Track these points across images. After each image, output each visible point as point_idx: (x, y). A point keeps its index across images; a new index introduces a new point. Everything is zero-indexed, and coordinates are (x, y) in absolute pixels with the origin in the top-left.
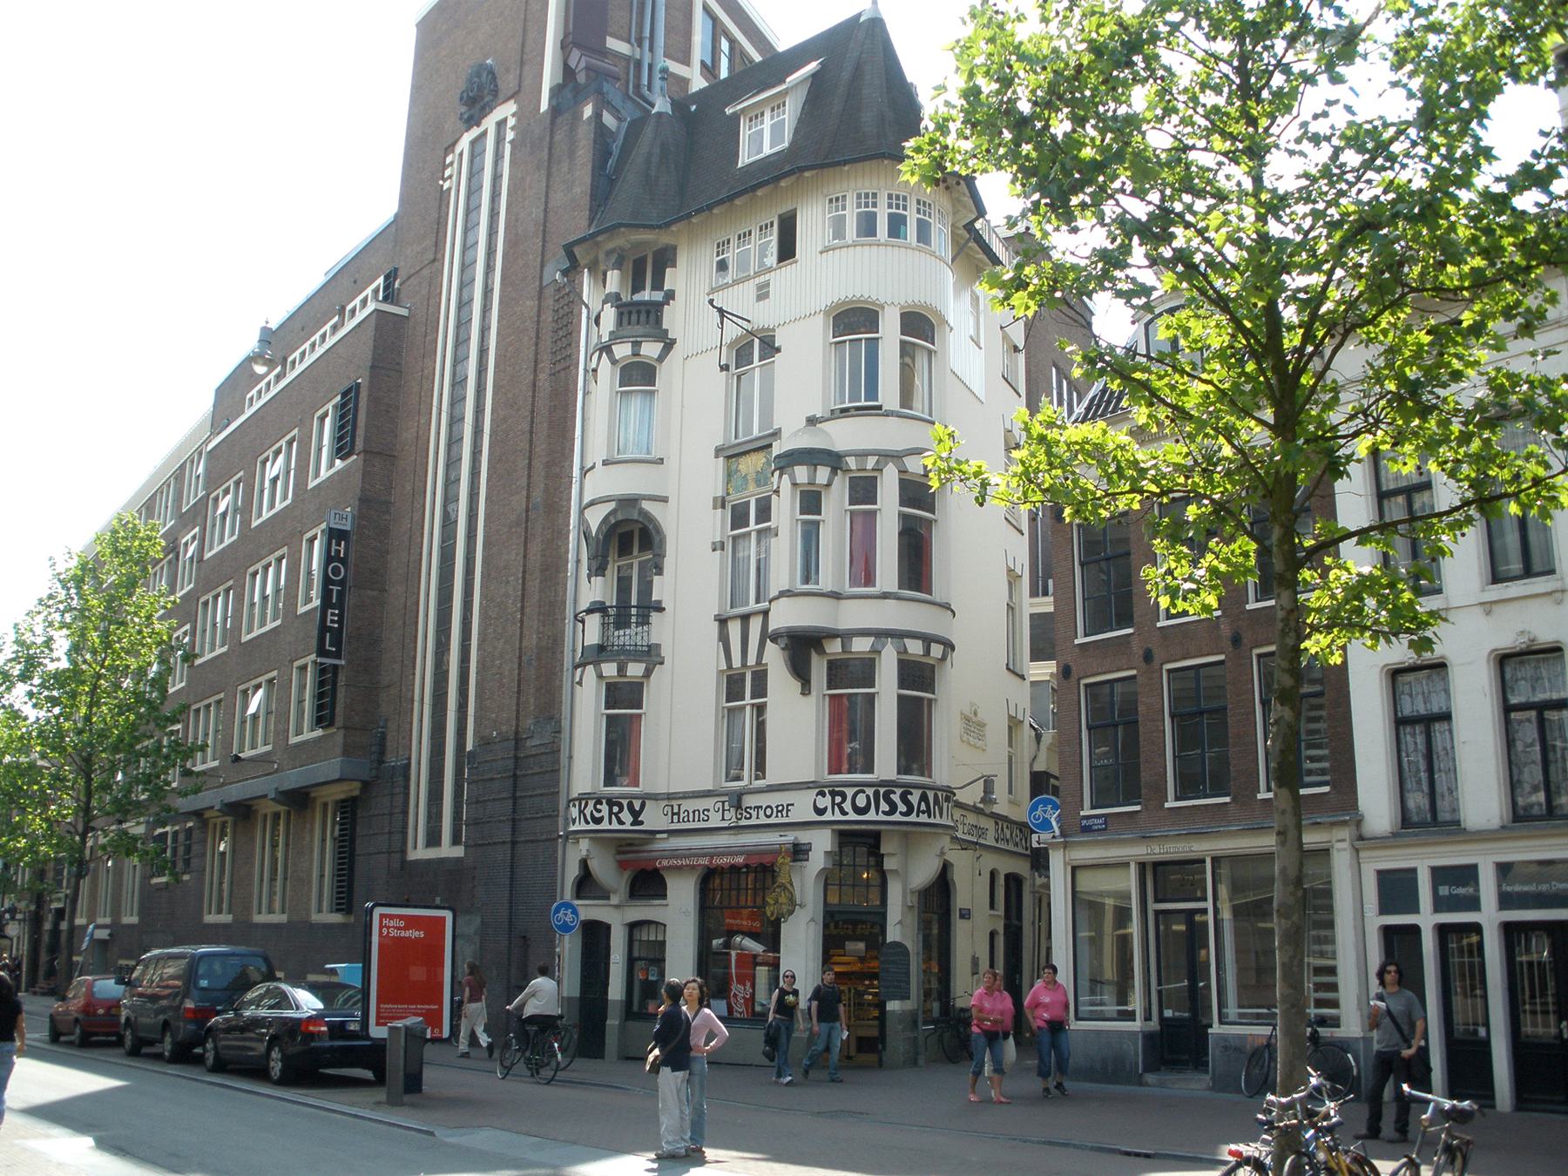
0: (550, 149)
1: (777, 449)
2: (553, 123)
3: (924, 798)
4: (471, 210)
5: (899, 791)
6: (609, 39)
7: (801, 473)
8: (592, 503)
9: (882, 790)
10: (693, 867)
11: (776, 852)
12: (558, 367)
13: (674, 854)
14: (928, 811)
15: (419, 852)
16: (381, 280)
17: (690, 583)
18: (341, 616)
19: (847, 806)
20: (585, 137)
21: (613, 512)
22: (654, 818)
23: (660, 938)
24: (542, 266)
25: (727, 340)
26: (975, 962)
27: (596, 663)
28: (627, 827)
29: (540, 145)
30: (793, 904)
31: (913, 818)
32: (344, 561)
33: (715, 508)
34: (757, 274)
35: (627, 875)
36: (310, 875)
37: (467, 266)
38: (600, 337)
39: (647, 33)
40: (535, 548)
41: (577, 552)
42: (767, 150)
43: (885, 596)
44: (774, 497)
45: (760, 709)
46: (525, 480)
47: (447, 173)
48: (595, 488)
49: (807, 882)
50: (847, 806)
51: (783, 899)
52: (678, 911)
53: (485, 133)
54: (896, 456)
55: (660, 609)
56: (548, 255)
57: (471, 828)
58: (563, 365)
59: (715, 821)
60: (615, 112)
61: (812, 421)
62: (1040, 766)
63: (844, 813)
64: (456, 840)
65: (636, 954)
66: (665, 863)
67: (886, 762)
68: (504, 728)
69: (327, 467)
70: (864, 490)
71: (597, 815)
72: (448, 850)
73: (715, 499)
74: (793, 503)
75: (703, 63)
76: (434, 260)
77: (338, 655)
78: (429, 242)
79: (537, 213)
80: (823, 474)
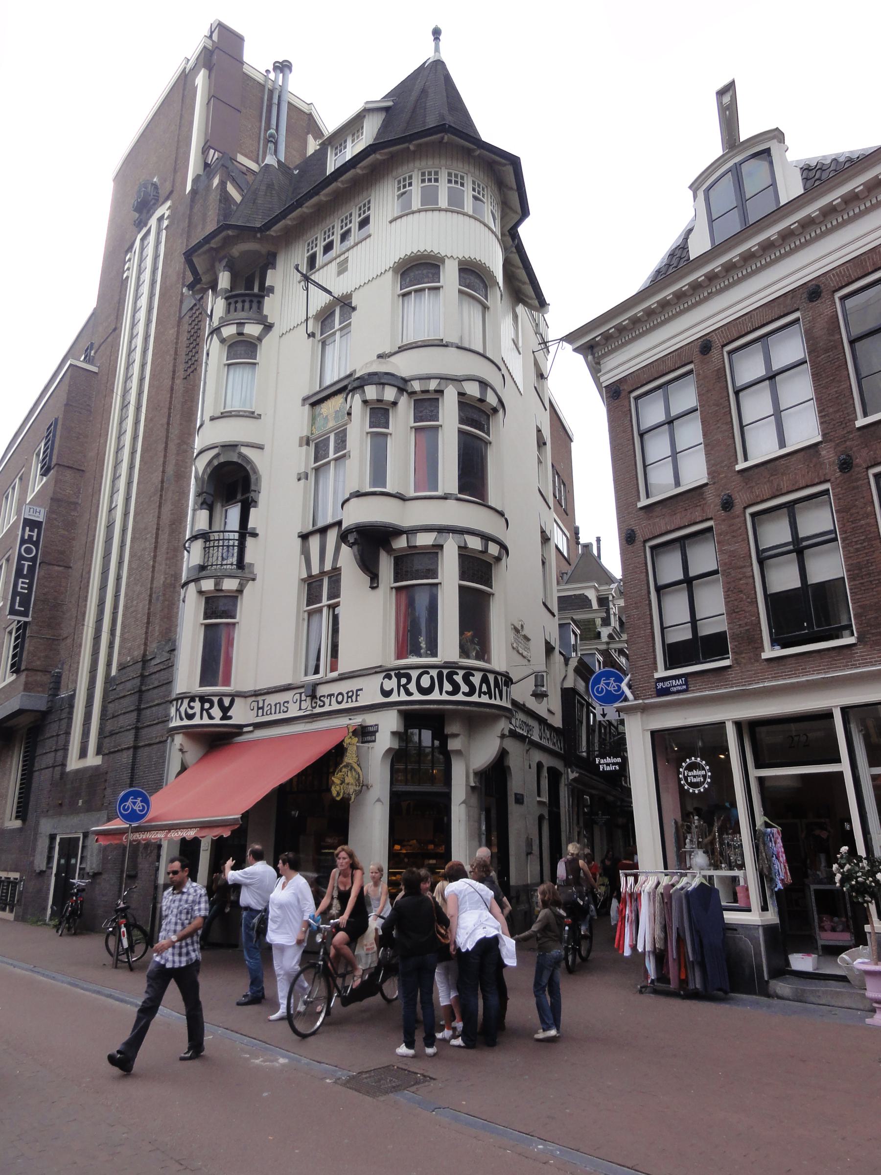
3: (485, 680)
5: (461, 673)
9: (445, 672)
14: (489, 693)
17: (281, 510)
18: (30, 586)
19: (412, 687)
20: (214, 198)
21: (217, 456)
25: (312, 312)
26: (529, 843)
28: (217, 721)
31: (475, 698)
32: (36, 544)
33: (301, 446)
36: (7, 792)
40: (167, 509)
43: (445, 497)
50: (412, 687)
51: (349, 779)
55: (255, 535)
62: (569, 684)
63: (409, 693)
70: (426, 405)
71: (190, 712)
73: (301, 438)
74: (363, 419)
76: (115, 330)
77: (25, 614)
80: (390, 394)
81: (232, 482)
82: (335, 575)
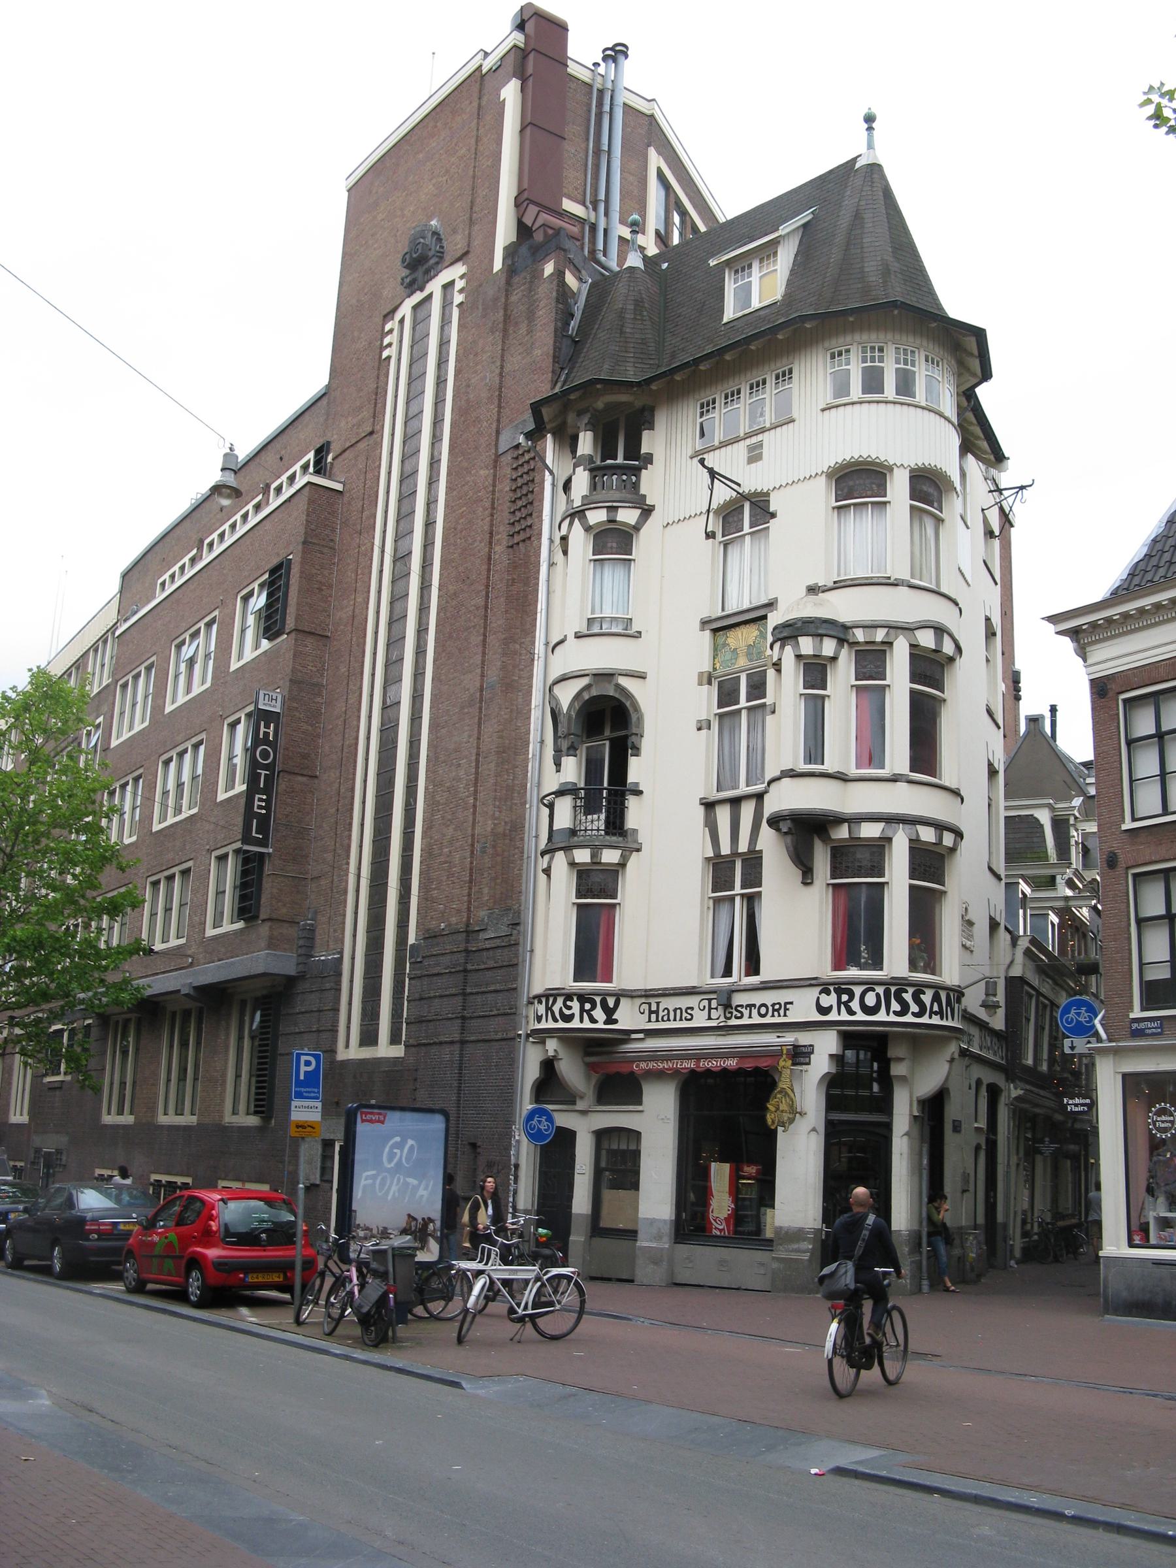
0: (506, 310)
1: (775, 619)
2: (508, 283)
3: (936, 998)
4: (416, 378)
5: (911, 990)
6: (564, 200)
7: (806, 645)
8: (564, 679)
9: (893, 989)
10: (677, 1072)
11: (774, 1054)
12: (517, 539)
13: (654, 1055)
14: (940, 1013)
15: (351, 1051)
16: (311, 456)
18: (268, 801)
19: (855, 1005)
20: (545, 295)
21: (587, 687)
22: (629, 1017)
23: (633, 1147)
24: (498, 432)
25: (714, 506)
26: (965, 1178)
27: (567, 849)
28: (600, 1025)
29: (495, 309)
30: (795, 1113)
31: (925, 1020)
32: (273, 744)
33: (700, 684)
34: (748, 436)
35: (595, 1078)
36: (224, 1075)
37: (411, 437)
38: (569, 501)
39: (602, 196)
40: (490, 728)
41: (540, 729)
42: (756, 304)
43: (895, 779)
44: (771, 673)
45: (751, 901)
46: (479, 658)
47: (386, 341)
48: (564, 659)
49: (808, 1090)
50: (855, 1005)
51: (783, 1107)
52: (657, 1120)
53: (430, 296)
54: (907, 629)
55: (638, 793)
56: (504, 421)
57: (416, 1026)
58: (522, 536)
59: (700, 1020)
60: (577, 272)
61: (812, 590)
62: (1016, 971)
63: (851, 1012)
64: (395, 1039)
65: (603, 1165)
66: (643, 1065)
67: (897, 959)
68: (454, 920)
69: (250, 647)
70: (871, 660)
71: (567, 1012)
72: (385, 1050)
73: (701, 674)
74: (797, 677)
75: (657, 233)
76: (372, 433)
77: (263, 843)
78: (366, 413)
79: (492, 377)
80: (829, 647)
81: (606, 722)
82: (753, 861)
